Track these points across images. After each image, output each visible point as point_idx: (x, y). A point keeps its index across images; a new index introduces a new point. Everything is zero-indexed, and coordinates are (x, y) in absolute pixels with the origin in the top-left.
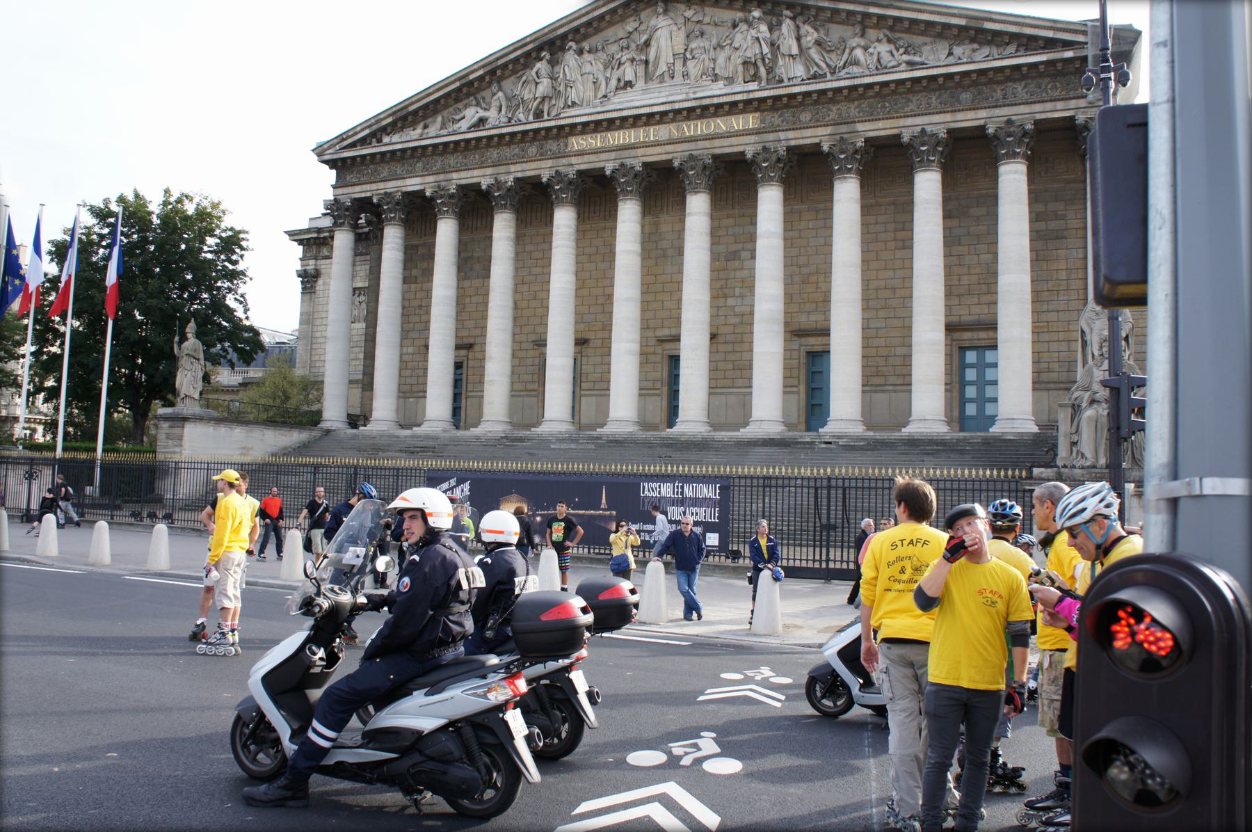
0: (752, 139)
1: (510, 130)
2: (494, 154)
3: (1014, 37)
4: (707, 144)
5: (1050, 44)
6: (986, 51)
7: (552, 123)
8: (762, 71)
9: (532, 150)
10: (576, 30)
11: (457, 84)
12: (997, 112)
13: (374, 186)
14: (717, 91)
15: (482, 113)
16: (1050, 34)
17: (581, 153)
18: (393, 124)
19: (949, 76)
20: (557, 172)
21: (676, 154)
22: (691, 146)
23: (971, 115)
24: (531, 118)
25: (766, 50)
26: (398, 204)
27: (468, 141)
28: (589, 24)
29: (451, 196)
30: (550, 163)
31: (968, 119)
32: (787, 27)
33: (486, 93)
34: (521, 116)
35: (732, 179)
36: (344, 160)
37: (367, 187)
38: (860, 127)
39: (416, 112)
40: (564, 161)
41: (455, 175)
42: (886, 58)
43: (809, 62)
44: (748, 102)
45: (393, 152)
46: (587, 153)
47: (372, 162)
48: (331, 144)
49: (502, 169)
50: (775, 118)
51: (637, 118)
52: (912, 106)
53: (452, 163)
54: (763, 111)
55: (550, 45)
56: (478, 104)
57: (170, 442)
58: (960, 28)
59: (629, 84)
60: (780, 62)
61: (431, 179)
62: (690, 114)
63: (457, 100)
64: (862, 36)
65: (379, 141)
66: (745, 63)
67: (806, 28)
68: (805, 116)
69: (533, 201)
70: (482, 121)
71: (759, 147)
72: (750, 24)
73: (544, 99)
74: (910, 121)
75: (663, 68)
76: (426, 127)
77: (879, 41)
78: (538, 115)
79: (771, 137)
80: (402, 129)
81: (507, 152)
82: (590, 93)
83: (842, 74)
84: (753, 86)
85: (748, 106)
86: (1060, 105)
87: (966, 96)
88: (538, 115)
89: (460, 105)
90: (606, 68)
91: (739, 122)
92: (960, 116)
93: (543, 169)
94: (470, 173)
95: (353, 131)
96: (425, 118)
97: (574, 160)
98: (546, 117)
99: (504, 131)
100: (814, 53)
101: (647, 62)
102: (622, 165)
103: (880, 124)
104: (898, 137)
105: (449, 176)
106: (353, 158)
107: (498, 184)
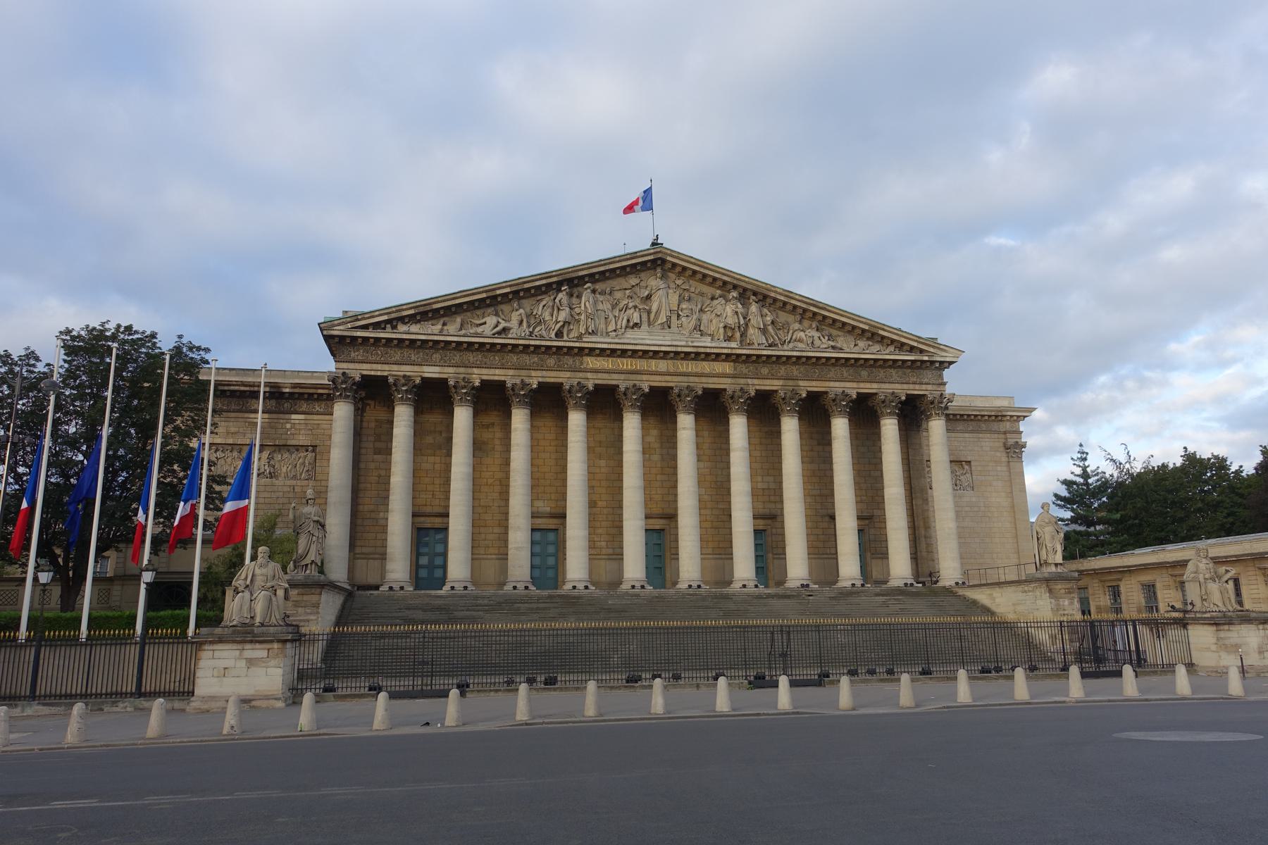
0: (729, 380)
1: (538, 343)
3: (893, 341)
4: (696, 379)
6: (877, 347)
7: (577, 345)
8: (738, 335)
9: (551, 361)
10: (592, 275)
11: (484, 295)
12: (883, 386)
13: (386, 367)
14: (706, 343)
15: (503, 324)
16: (915, 344)
17: (596, 371)
18: (412, 317)
19: (857, 360)
20: (579, 383)
22: (685, 379)
23: (868, 385)
24: (553, 336)
25: (742, 322)
26: (415, 386)
27: (493, 345)
28: (603, 273)
29: (473, 388)
30: (568, 374)
32: (754, 308)
33: (506, 308)
34: (544, 333)
36: (356, 338)
37: (379, 367)
38: (801, 383)
39: (438, 310)
40: (581, 375)
41: (476, 371)
42: (817, 342)
44: (728, 355)
45: (415, 341)
47: (385, 345)
48: (342, 321)
49: (524, 373)
50: (743, 368)
51: (645, 352)
52: (831, 374)
53: (471, 359)
54: (734, 361)
55: (572, 282)
56: (497, 315)
57: (300, 610)
58: (864, 331)
59: (636, 325)
60: (751, 331)
61: (451, 370)
63: (478, 308)
64: (800, 322)
65: (394, 327)
66: (725, 327)
67: (765, 310)
68: (765, 371)
70: (505, 330)
71: (738, 387)
72: (727, 301)
73: (566, 323)
74: (832, 384)
75: (662, 319)
76: (444, 324)
77: (810, 327)
78: (559, 334)
79: (742, 381)
80: (419, 321)
81: (527, 359)
82: (602, 326)
83: (791, 345)
84: (733, 345)
86: (917, 387)
87: (864, 373)
89: (479, 312)
90: (614, 307)
91: (719, 367)
92: (862, 385)
94: (492, 371)
95: (371, 314)
96: (443, 316)
97: (589, 375)
98: (565, 338)
99: (532, 343)
100: (770, 328)
101: (649, 312)
102: (634, 386)
103: (814, 383)
104: (826, 393)
105: (470, 370)
106: (366, 339)
107: (524, 385)
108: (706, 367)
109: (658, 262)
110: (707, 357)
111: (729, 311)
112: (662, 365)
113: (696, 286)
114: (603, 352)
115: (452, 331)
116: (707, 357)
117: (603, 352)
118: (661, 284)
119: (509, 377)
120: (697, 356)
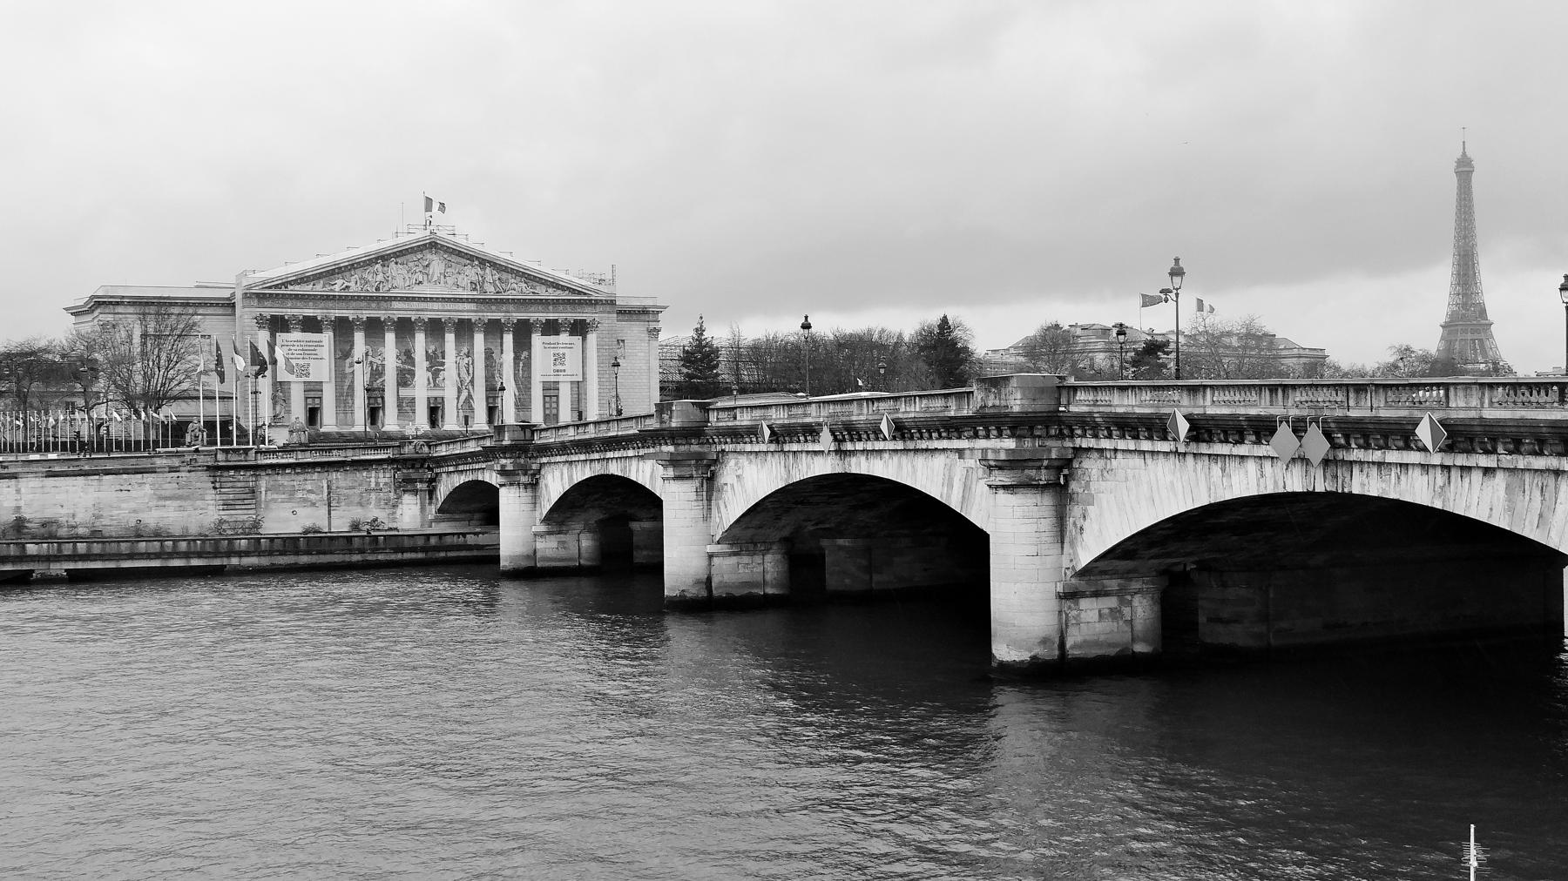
2: (354, 304)
5: (580, 293)
14: (460, 291)
21: (444, 316)
31: (552, 316)
35: (464, 329)
43: (495, 286)
46: (399, 311)
55: (383, 258)
62: (449, 300)
69: (374, 328)
78: (377, 289)
85: (473, 301)
88: (377, 289)
91: (467, 306)
93: (381, 314)
107: (358, 319)
108: (460, 306)
109: (433, 246)
110: (461, 300)
111: (472, 273)
112: (436, 306)
113: (454, 258)
114: (402, 299)
115: (318, 288)
116: (461, 300)
117: (402, 299)
118: (434, 257)
119: (350, 314)
120: (455, 300)
